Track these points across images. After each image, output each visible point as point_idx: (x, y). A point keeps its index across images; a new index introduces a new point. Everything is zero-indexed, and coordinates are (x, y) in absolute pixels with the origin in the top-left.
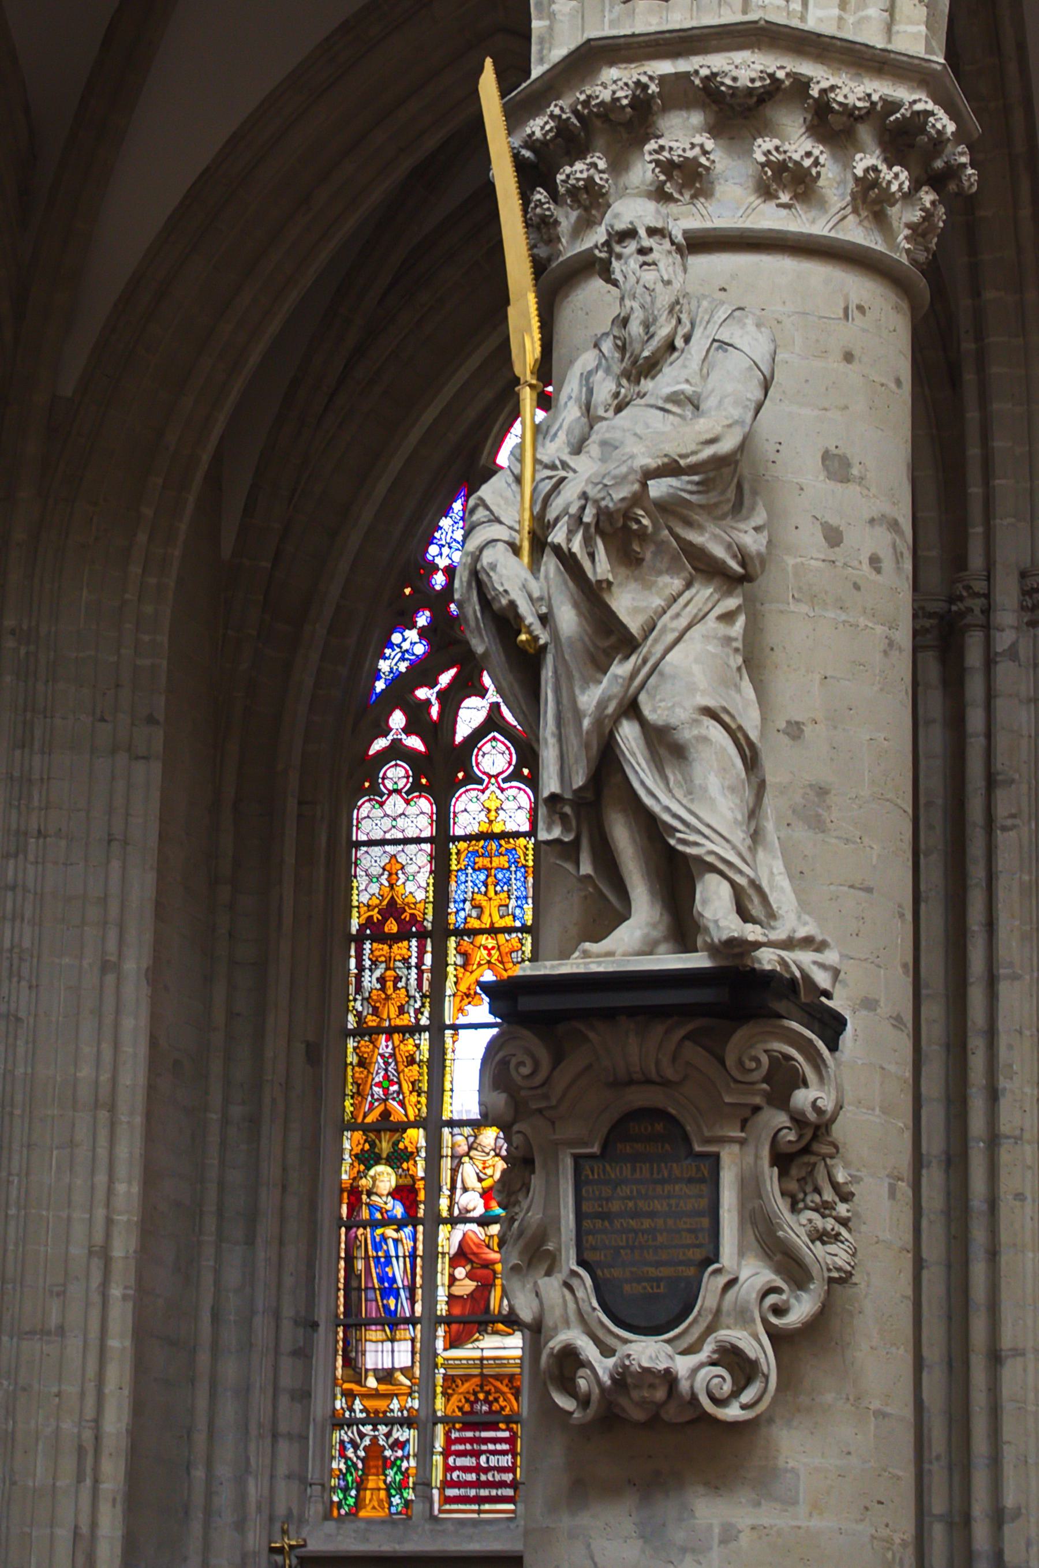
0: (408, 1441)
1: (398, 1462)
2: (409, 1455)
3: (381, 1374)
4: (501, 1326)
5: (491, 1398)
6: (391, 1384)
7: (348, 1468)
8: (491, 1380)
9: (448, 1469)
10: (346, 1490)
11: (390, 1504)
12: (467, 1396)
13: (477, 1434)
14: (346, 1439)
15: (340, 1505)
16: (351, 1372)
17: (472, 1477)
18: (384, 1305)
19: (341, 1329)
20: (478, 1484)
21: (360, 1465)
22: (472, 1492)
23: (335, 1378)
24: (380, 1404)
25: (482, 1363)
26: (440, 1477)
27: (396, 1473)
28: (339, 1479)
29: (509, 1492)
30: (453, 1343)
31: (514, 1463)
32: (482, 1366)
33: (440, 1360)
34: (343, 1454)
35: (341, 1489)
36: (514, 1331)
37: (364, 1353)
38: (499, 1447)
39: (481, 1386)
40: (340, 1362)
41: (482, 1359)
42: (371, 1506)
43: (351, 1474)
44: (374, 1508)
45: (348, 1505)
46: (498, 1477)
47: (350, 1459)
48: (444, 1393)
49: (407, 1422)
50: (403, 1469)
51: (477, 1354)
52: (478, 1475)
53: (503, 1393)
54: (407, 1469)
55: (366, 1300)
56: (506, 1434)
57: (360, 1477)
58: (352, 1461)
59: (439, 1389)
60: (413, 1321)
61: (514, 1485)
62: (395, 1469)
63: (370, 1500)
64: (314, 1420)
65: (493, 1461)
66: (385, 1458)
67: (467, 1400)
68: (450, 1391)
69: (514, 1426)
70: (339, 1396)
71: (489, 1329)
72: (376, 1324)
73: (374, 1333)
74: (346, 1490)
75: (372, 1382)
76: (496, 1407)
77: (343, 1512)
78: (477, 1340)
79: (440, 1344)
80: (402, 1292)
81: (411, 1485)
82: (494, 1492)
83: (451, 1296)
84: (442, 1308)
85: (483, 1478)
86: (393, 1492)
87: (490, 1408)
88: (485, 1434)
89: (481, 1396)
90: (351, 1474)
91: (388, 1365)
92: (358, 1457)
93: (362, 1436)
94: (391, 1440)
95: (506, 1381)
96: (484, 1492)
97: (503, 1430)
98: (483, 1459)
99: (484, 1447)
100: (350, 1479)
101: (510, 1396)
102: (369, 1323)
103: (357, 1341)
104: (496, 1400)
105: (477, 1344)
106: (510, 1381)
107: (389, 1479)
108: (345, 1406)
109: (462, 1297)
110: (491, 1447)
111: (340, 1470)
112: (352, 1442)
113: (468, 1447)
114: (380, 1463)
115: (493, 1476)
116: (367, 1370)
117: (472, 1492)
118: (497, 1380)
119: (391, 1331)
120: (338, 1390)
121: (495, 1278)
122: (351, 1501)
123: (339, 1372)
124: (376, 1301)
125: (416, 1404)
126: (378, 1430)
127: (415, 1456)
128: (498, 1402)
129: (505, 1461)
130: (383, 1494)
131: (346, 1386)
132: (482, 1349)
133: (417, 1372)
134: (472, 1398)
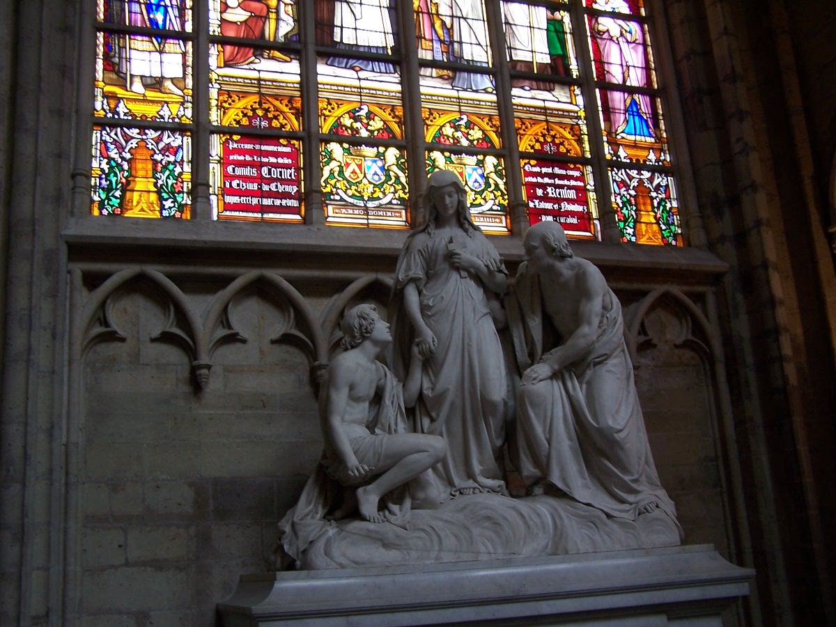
0: (181, 147)
1: (171, 167)
2: (182, 160)
3: (149, 81)
4: (277, 54)
5: (270, 115)
6: (161, 92)
7: (111, 168)
8: (270, 99)
9: (226, 176)
10: (109, 190)
11: (162, 208)
12: (245, 111)
13: (257, 147)
14: (108, 139)
15: (101, 205)
16: (114, 76)
17: (254, 187)
18: (150, 19)
19: (101, 35)
20: (261, 194)
21: (126, 166)
22: (255, 201)
23: (95, 80)
24: (150, 111)
25: (259, 84)
26: (218, 183)
27: (168, 177)
28: (101, 179)
29: (294, 203)
30: (227, 64)
31: (298, 176)
32: (259, 86)
33: (214, 76)
34: (105, 155)
35: (103, 189)
36: (291, 59)
37: (129, 60)
38: (280, 161)
39: (260, 104)
40: (100, 65)
41: (259, 80)
42: (139, 208)
43: (116, 175)
44: (142, 210)
45: (112, 206)
46: (281, 189)
47: (113, 159)
48: (219, 107)
49: (179, 129)
50: (176, 174)
51: (255, 75)
52: (260, 184)
53: (282, 112)
54: (181, 174)
55: (130, 12)
56: (288, 150)
57: (126, 178)
58: (116, 162)
59: (214, 103)
60: (181, 36)
61: (298, 196)
62: (167, 173)
63: (138, 203)
64: (77, 112)
65: (275, 173)
66: (155, 162)
67: (245, 115)
68: (226, 105)
69: (295, 142)
70: (100, 98)
71: (266, 55)
72: (142, 35)
73: (140, 43)
74: (109, 190)
75: (138, 87)
76: (275, 123)
77: (105, 212)
78: (251, 63)
79: (213, 62)
80: (170, 9)
81: (185, 190)
82: (278, 202)
83: (223, 20)
84: (214, 28)
85: (265, 188)
86: (165, 196)
87: (270, 123)
88: (264, 148)
89: (260, 113)
90: (116, 175)
91: (157, 74)
92: (123, 159)
93: (128, 139)
94: (161, 145)
95: (285, 102)
96: (267, 202)
97: (284, 146)
98: (265, 170)
99: (265, 160)
100: (114, 180)
101: (293, 118)
102: (135, 32)
103: (119, 47)
104: (276, 117)
105: (252, 66)
106: (289, 102)
107: (160, 182)
108: (106, 107)
109: (236, 23)
110: (273, 160)
111: (102, 170)
112: (115, 142)
113: (248, 158)
114: (150, 166)
115: (277, 187)
116: (132, 76)
117: (255, 201)
118: (277, 100)
119: (159, 44)
120: (98, 92)
121: (269, 12)
122: (115, 202)
123: (99, 75)
124: (142, 13)
125: (189, 113)
126: (146, 134)
127: (188, 162)
128: (278, 120)
129: (287, 174)
130: (153, 197)
131: (108, 88)
132: (259, 71)
133: (189, 82)
134: (250, 114)
